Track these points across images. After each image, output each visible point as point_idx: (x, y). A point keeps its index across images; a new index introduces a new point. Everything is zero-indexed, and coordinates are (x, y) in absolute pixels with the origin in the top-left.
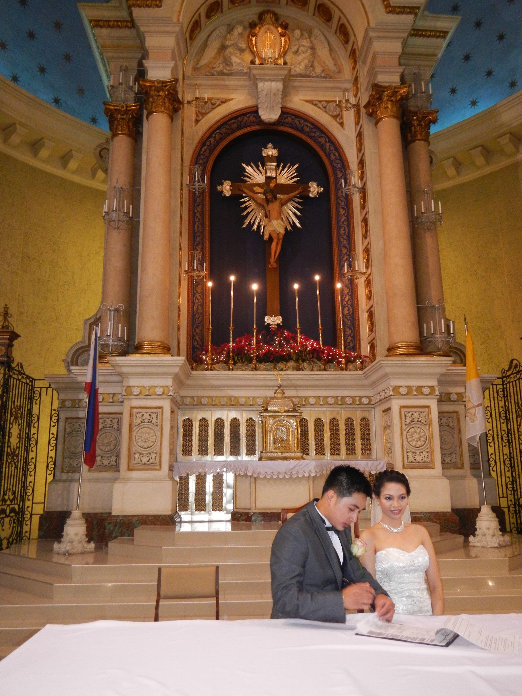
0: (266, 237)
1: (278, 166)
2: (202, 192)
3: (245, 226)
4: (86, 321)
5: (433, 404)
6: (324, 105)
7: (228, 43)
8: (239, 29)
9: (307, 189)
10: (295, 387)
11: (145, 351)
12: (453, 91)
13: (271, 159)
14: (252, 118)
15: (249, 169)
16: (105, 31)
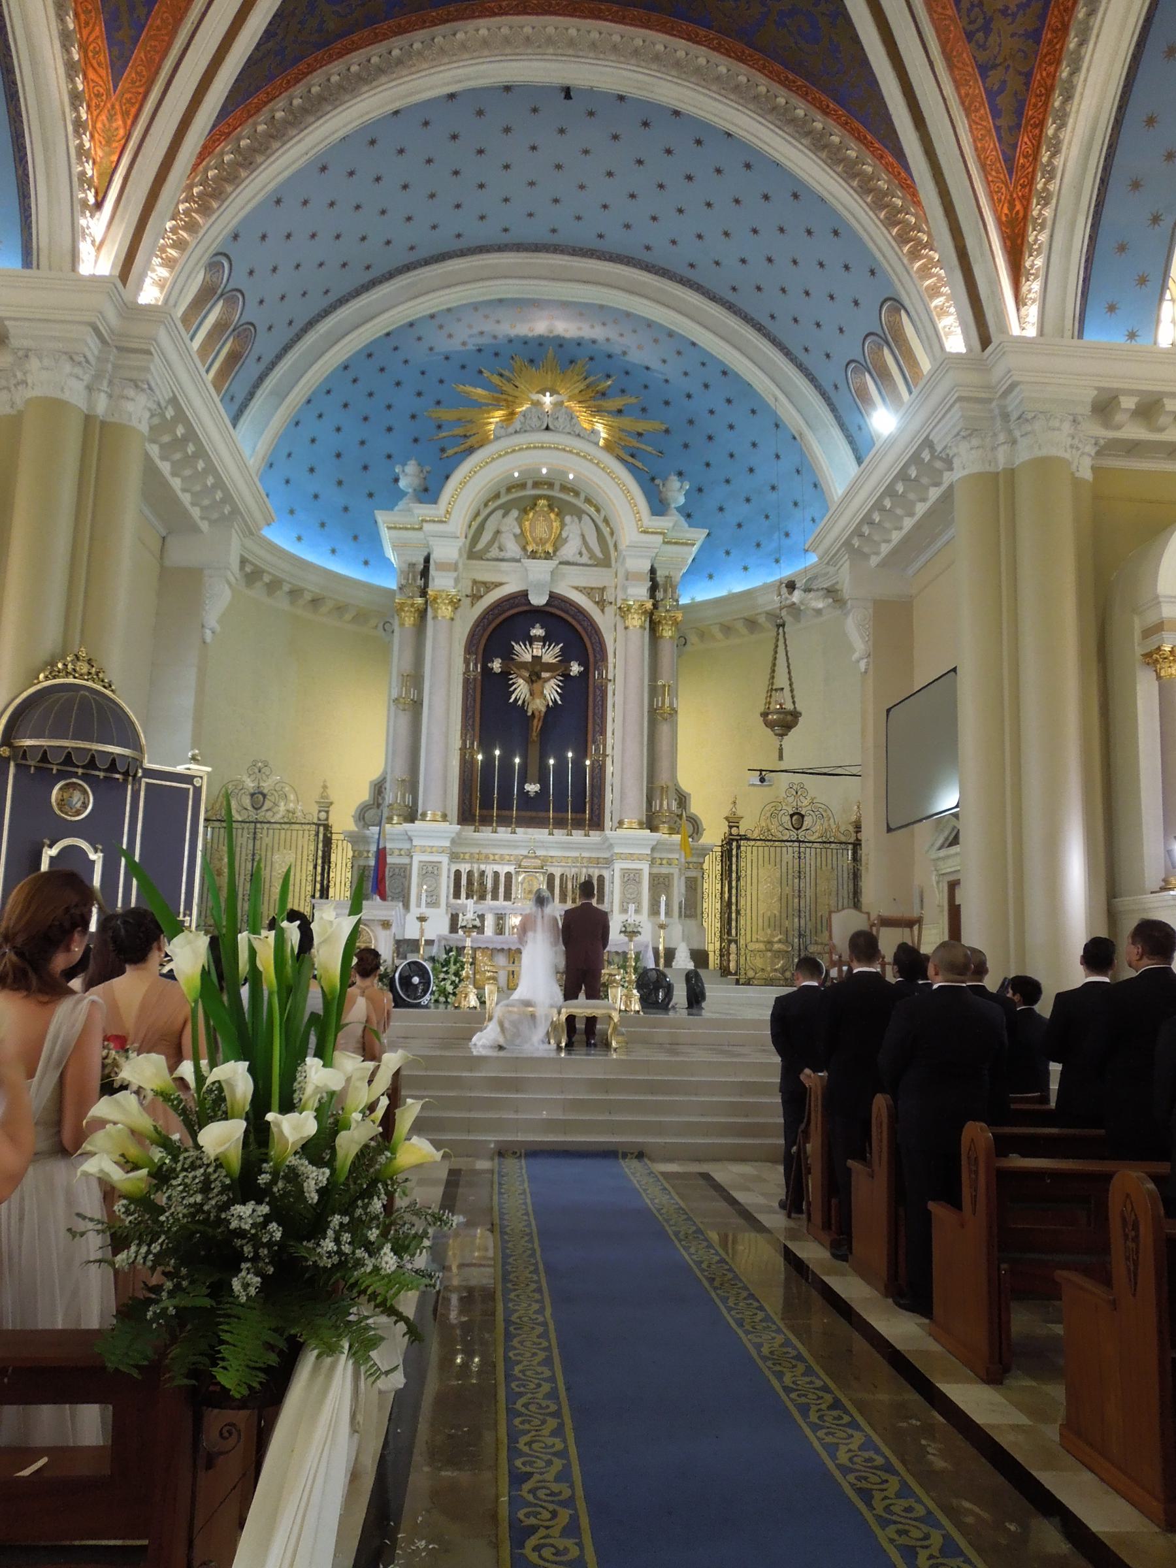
0: (529, 714)
1: (544, 646)
2: (475, 679)
3: (511, 701)
4: (371, 782)
5: (645, 867)
6: (588, 591)
7: (503, 529)
8: (515, 513)
9: (568, 668)
10: (547, 848)
11: (428, 819)
12: (728, 553)
13: (537, 638)
14: (523, 601)
15: (516, 647)
16: (394, 532)
